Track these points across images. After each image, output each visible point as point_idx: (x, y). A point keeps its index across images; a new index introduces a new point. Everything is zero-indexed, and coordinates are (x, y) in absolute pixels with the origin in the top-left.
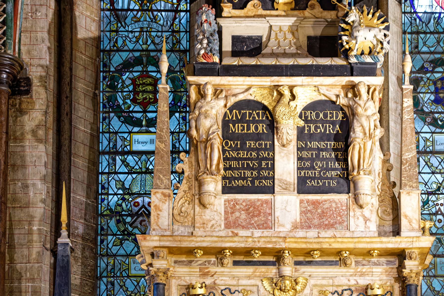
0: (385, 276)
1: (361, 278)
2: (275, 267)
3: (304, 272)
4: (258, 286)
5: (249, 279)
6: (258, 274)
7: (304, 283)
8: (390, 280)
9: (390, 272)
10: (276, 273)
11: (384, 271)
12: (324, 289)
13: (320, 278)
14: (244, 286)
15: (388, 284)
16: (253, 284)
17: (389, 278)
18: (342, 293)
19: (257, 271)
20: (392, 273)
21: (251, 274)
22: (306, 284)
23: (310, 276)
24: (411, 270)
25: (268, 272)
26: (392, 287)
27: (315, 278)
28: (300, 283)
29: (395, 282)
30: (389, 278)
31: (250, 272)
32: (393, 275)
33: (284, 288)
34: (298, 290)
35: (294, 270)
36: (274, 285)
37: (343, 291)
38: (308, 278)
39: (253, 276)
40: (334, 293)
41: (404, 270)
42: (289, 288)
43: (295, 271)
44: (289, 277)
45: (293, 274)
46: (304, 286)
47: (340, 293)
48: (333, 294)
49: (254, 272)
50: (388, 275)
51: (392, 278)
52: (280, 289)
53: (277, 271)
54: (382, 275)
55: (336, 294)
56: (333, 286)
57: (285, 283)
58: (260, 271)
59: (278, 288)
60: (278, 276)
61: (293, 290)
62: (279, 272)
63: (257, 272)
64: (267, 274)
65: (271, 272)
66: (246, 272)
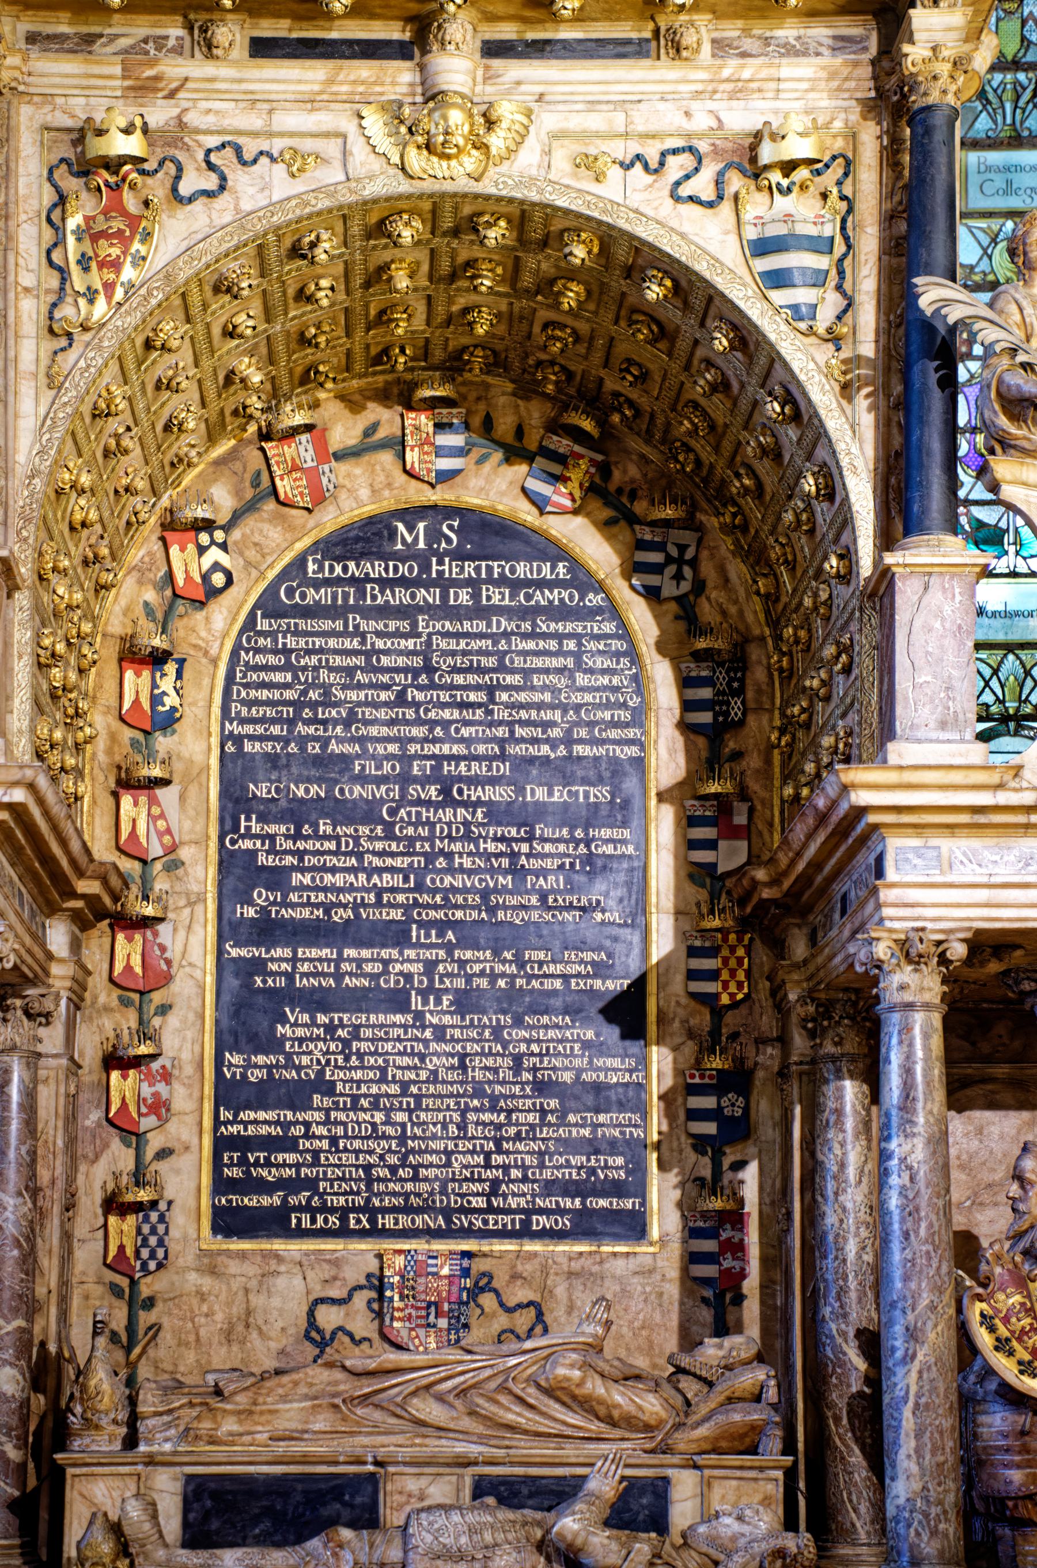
0: (825, 95)
1: (734, 103)
2: (408, 64)
3: (519, 83)
4: (345, 137)
5: (312, 110)
6: (345, 88)
7: (517, 127)
8: (846, 110)
9: (846, 79)
10: (412, 85)
11: (823, 74)
12: (592, 151)
13: (580, 107)
14: (292, 134)
15: (838, 125)
16: (324, 128)
17: (840, 103)
18: (662, 164)
19: (341, 77)
20: (852, 84)
21: (316, 88)
22: (526, 128)
23: (540, 98)
24: (934, 49)
25: (382, 84)
26: (853, 137)
27: (561, 107)
28: (504, 125)
29: (865, 119)
30: (840, 103)
31: (312, 82)
32: (856, 90)
33: (441, 139)
34: (494, 151)
35: (480, 73)
36: (403, 130)
37: (663, 154)
38: (534, 106)
39: (325, 97)
40: (632, 164)
41: (906, 48)
42: (461, 142)
43: (486, 80)
44: (463, 96)
45: (478, 89)
46: (518, 139)
47: (653, 164)
48: (626, 166)
49: (330, 81)
50: (839, 89)
51: (854, 103)
52: (429, 147)
53: (418, 80)
54: (812, 90)
55: (638, 167)
56: (626, 135)
57: (445, 118)
58: (352, 77)
59: (420, 140)
60: (419, 99)
61: (474, 152)
62: (423, 84)
63: (342, 83)
64: (378, 89)
65: (394, 83)
66: (300, 82)
